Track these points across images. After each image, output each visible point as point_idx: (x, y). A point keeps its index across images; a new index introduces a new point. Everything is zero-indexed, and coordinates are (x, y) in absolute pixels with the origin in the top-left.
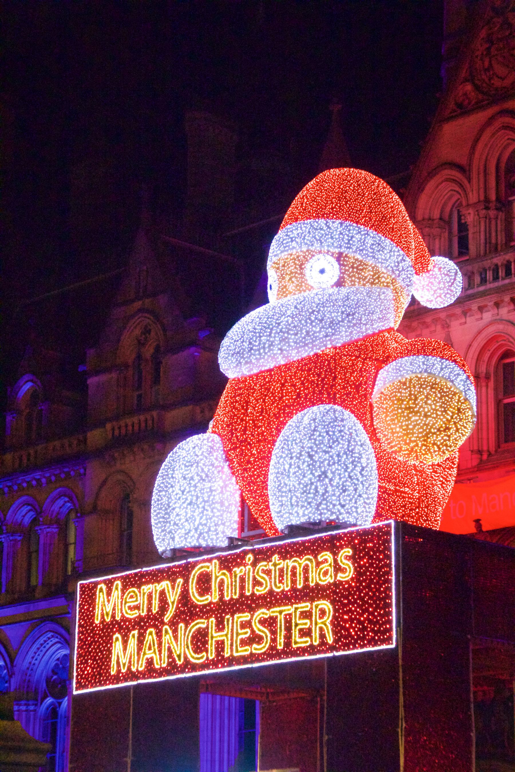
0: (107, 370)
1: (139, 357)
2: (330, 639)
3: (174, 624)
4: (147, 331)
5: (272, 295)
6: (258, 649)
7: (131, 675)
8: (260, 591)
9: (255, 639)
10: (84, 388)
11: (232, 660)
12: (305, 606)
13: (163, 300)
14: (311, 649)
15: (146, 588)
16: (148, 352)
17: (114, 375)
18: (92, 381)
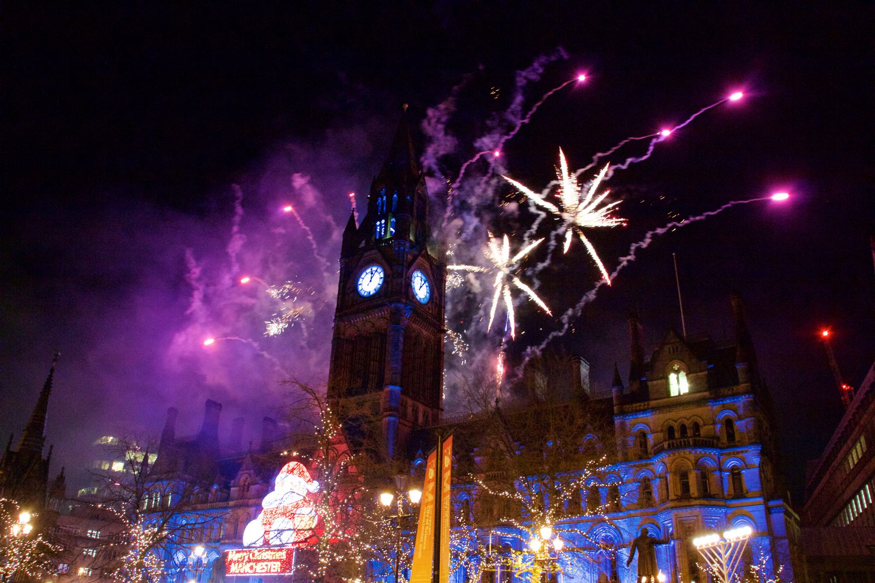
0: (237, 487)
1: (244, 484)
2: (279, 571)
3: (246, 563)
4: (247, 478)
5: (276, 488)
6: (263, 571)
7: (235, 573)
8: (265, 558)
9: (264, 569)
10: (230, 490)
11: (257, 573)
12: (275, 563)
13: (252, 471)
14: (275, 573)
15: (241, 554)
16: (247, 484)
17: (238, 488)
18: (232, 489)
